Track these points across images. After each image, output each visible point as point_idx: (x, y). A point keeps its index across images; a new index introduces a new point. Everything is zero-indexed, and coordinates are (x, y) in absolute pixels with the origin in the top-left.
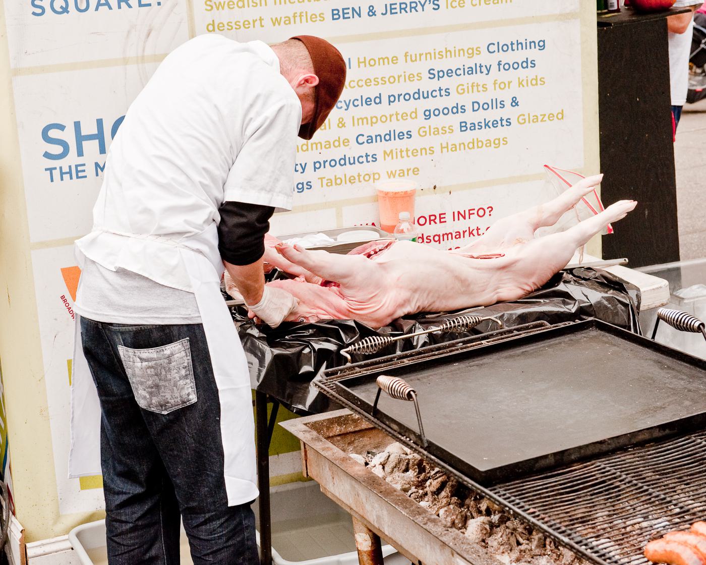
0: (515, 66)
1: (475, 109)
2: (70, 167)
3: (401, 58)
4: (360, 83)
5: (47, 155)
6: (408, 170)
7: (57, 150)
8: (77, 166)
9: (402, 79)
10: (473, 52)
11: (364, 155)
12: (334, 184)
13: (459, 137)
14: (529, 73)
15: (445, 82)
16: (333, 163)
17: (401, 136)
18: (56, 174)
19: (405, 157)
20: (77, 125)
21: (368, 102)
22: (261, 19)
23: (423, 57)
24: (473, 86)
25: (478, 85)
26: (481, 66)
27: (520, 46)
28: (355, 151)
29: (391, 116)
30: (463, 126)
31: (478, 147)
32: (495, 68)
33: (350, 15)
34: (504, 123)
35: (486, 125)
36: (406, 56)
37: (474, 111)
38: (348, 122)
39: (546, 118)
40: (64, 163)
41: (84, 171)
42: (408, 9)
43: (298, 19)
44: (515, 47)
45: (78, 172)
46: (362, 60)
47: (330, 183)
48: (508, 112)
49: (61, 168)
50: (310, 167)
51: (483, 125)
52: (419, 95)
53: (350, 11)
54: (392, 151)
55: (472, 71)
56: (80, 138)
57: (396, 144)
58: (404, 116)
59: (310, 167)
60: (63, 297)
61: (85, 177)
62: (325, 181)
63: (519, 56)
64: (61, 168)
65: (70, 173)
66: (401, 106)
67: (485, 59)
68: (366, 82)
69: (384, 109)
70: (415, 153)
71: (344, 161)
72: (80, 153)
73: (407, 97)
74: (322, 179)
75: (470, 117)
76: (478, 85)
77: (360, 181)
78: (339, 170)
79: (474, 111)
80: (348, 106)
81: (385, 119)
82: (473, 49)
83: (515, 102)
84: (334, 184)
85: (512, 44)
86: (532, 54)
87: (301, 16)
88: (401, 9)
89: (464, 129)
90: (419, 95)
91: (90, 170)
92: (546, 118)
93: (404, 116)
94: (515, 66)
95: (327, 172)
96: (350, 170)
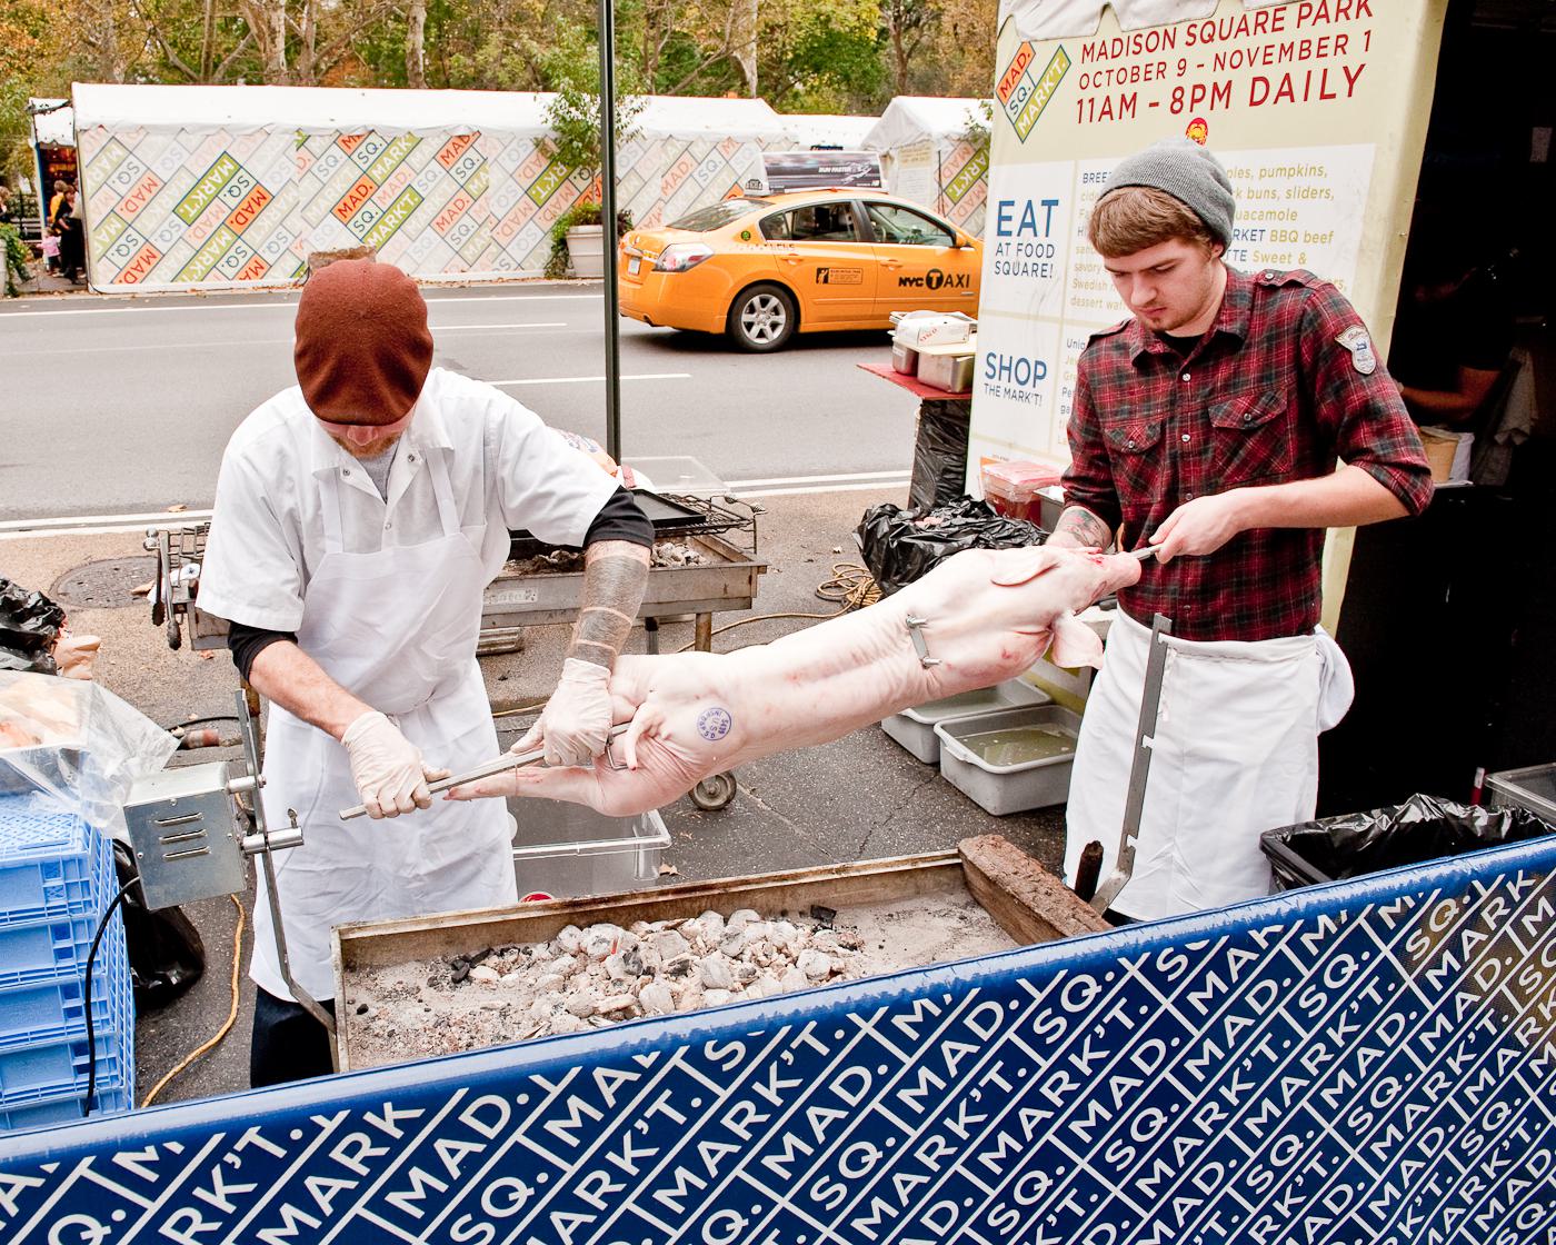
7: (991, 373)
56: (1002, 368)
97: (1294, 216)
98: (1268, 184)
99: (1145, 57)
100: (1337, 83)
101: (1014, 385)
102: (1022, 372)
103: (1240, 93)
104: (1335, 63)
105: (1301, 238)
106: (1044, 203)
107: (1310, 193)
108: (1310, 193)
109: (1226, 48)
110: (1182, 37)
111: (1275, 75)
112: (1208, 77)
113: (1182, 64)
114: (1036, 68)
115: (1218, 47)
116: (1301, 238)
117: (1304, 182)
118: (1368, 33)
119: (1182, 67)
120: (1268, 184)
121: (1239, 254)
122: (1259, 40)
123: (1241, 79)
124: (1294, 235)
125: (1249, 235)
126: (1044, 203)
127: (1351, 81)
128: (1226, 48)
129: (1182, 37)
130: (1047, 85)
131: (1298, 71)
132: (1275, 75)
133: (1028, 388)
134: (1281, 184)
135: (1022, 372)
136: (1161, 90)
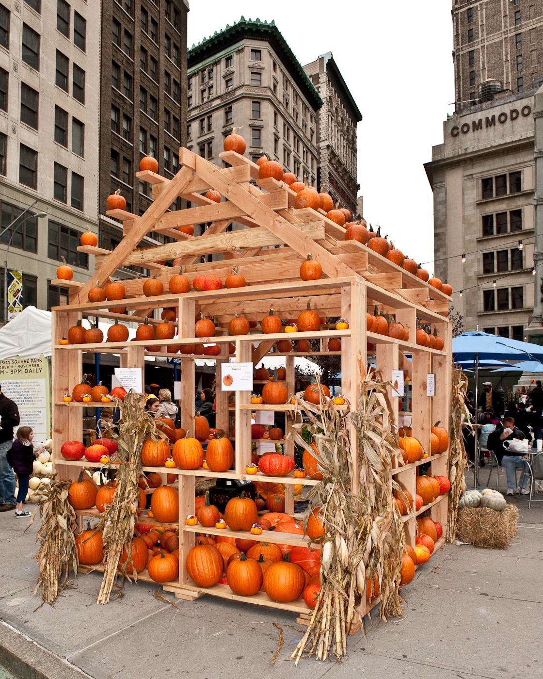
10: (30, 412)
15: (26, 416)
48: (35, 422)
63: (37, 413)
75: (29, 422)
86: (39, 413)
99: (4, 365)
100: (38, 370)
103: (23, 371)
104: (38, 368)
109: (20, 364)
110: (11, 362)
111: (29, 369)
112: (17, 369)
115: (18, 364)
117: (35, 384)
119: (12, 367)
122: (25, 364)
123: (23, 369)
128: (20, 364)
129: (11, 362)
132: (29, 369)
134: (32, 384)
136: (9, 370)
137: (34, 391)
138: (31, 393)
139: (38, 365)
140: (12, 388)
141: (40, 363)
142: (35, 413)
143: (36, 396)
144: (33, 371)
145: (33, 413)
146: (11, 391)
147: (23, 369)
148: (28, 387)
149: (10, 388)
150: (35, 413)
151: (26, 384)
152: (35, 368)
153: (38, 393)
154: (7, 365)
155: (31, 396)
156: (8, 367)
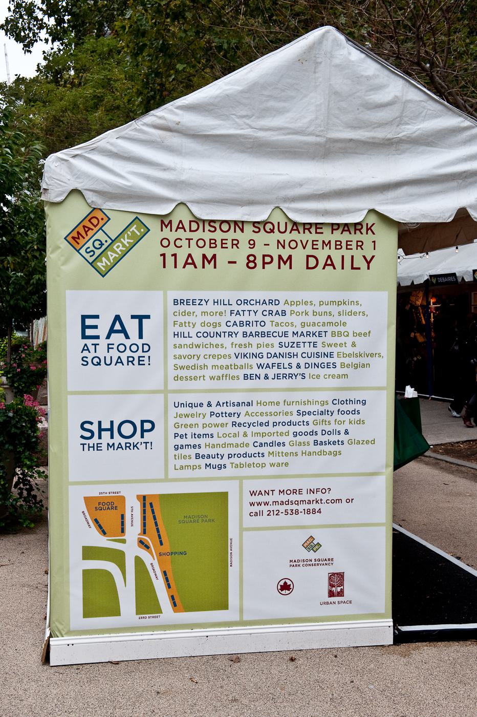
0: (348, 412)
1: (323, 434)
2: (94, 444)
3: (282, 403)
4: (257, 414)
5: (82, 437)
6: (282, 464)
7: (88, 434)
8: (97, 444)
9: (281, 414)
10: (323, 403)
11: (257, 453)
12: (239, 467)
13: (312, 448)
14: (357, 417)
15: (307, 418)
16: (239, 456)
17: (279, 444)
18: (86, 447)
19: (281, 456)
20: (100, 423)
21: (261, 424)
22: (204, 376)
23: (294, 403)
24: (322, 421)
25: (325, 421)
26: (328, 411)
27: (351, 402)
28: (251, 450)
29: (274, 433)
30: (316, 443)
31: (324, 455)
32: (336, 412)
33: (254, 378)
34: (340, 443)
35: (329, 443)
36: (284, 402)
37: (322, 435)
38: (249, 434)
39: (365, 442)
40: (91, 442)
41: (101, 447)
42: (287, 377)
43: (224, 378)
44: (348, 402)
45: (98, 447)
46: (259, 402)
47: (237, 466)
48: (342, 437)
49: (89, 444)
50: (226, 457)
51: (327, 443)
52: (290, 423)
53: (254, 376)
54: (273, 452)
55: (323, 413)
56: (101, 430)
57: (275, 449)
58: (282, 434)
59: (226, 457)
60: (83, 512)
61: (101, 450)
62: (234, 465)
63: (351, 407)
64: (89, 444)
65: (93, 447)
66: (280, 429)
67: (330, 407)
68: (260, 414)
69: (270, 429)
70: (287, 454)
71: (245, 455)
72: (100, 437)
73: (284, 424)
74: (232, 463)
75: (320, 438)
76: (325, 421)
77: (254, 467)
78: (242, 460)
79: (322, 435)
80: (249, 426)
81: (270, 434)
82: (324, 402)
83: (346, 432)
84: (239, 467)
85: (347, 401)
86: (358, 407)
87: (226, 376)
88: (283, 377)
89: (316, 444)
90: (290, 423)
91: (104, 446)
92: (365, 442)
93: (282, 434)
94: (348, 412)
95: (236, 460)
96: (248, 460)
97: (344, 324)
98: (324, 308)
101: (117, 439)
102: (127, 429)
104: (358, 254)
105: (351, 334)
106: (133, 317)
107: (351, 313)
108: (351, 313)
111: (322, 255)
113: (252, 242)
114: (113, 229)
115: (277, 236)
116: (351, 334)
118: (374, 242)
119: (252, 244)
120: (324, 308)
121: (312, 344)
123: (299, 256)
124: (346, 334)
125: (317, 334)
126: (133, 317)
127: (369, 263)
130: (126, 241)
131: (336, 256)
132: (322, 255)
133: (137, 438)
134: (334, 309)
135: (127, 429)
137: (340, 334)
138: (329, 339)
139: (360, 244)
140: (252, 318)
141: (367, 238)
142: (344, 407)
143: (349, 350)
144: (338, 264)
145: (335, 408)
146: (248, 329)
147: (299, 256)
148: (317, 319)
149: (245, 318)
150: (344, 407)
151: (309, 309)
152: (348, 255)
153: (357, 340)
154: (231, 235)
155: (327, 350)
156: (235, 243)
